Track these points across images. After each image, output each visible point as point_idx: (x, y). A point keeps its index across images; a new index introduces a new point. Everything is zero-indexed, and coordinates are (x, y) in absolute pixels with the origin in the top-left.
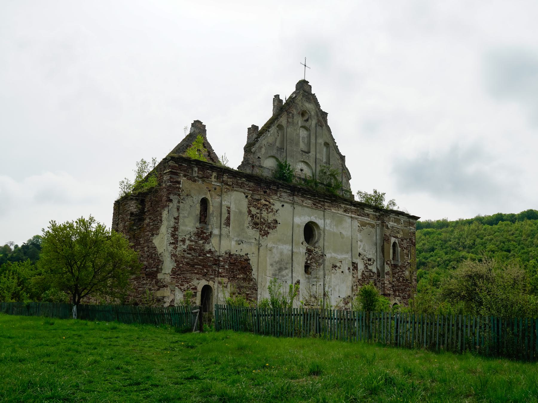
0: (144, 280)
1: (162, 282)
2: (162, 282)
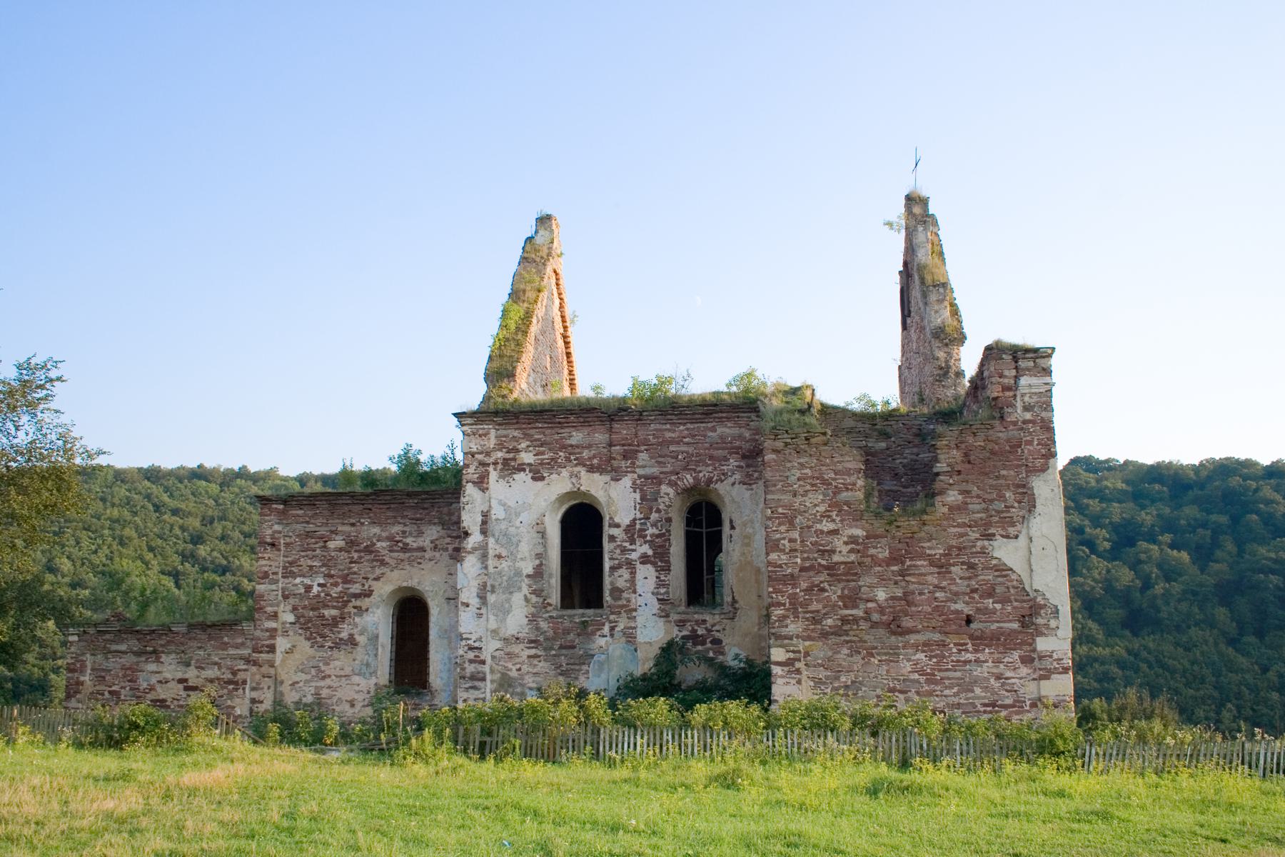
0: (967, 650)
1: (1062, 659)
2: (1062, 659)
